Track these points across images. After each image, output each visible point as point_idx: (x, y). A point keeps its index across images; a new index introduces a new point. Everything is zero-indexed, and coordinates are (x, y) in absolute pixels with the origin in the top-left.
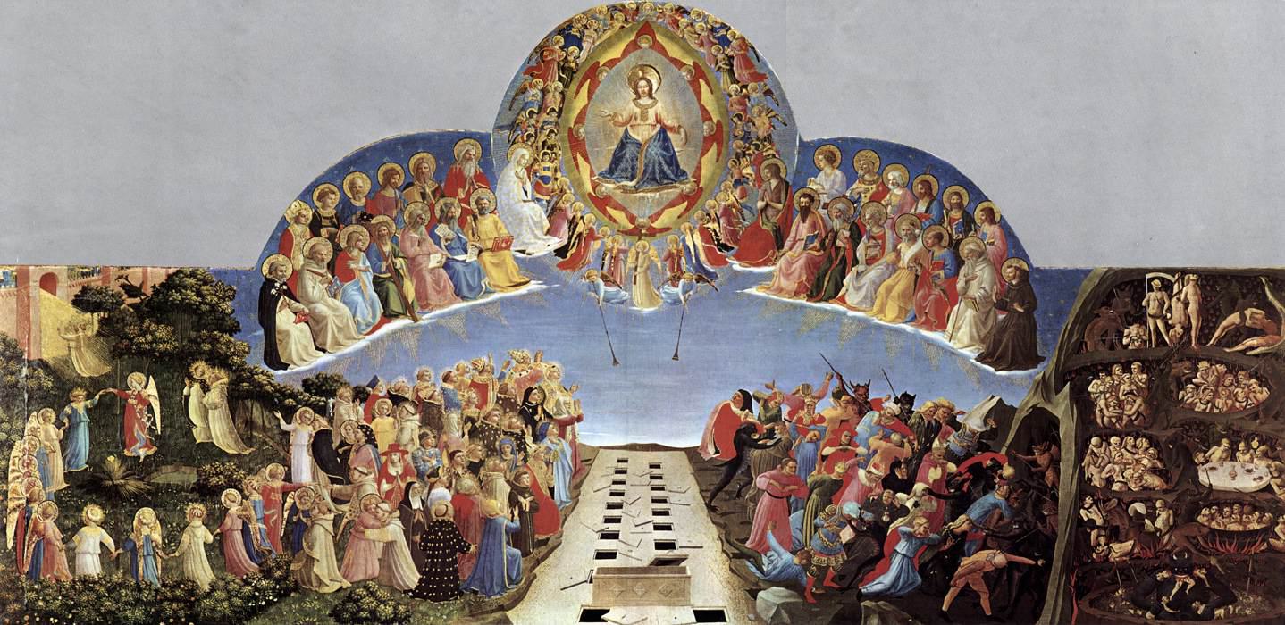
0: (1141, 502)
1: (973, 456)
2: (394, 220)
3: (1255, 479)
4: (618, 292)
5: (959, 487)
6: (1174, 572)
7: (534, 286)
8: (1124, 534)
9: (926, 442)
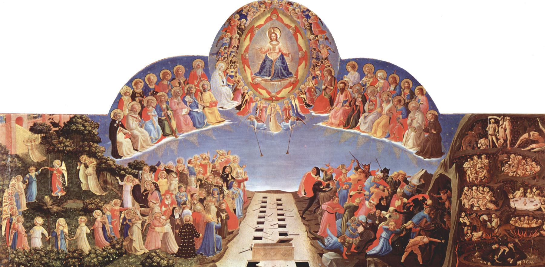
0: (486, 215)
1: (414, 195)
2: (167, 94)
3: (534, 205)
4: (263, 125)
5: (408, 208)
6: (500, 245)
7: (227, 122)
8: (478, 229)
9: (394, 190)
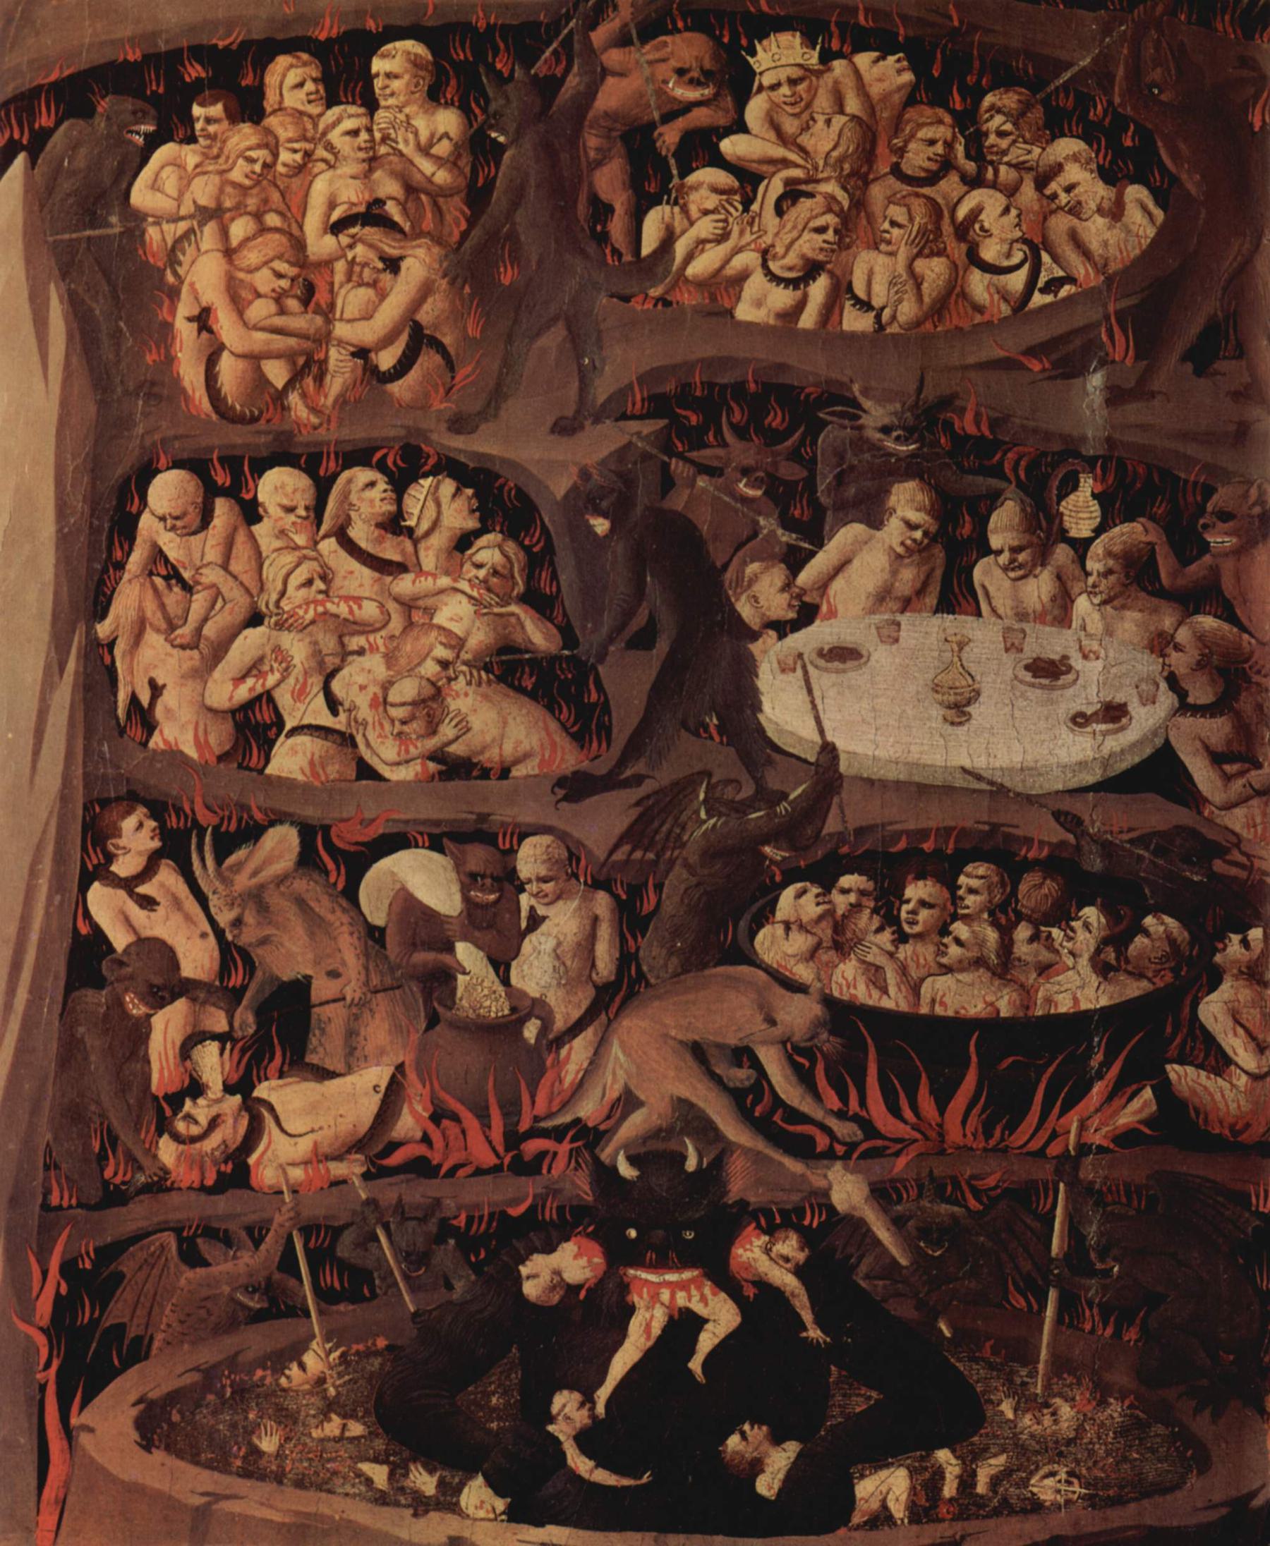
0: (436, 845)
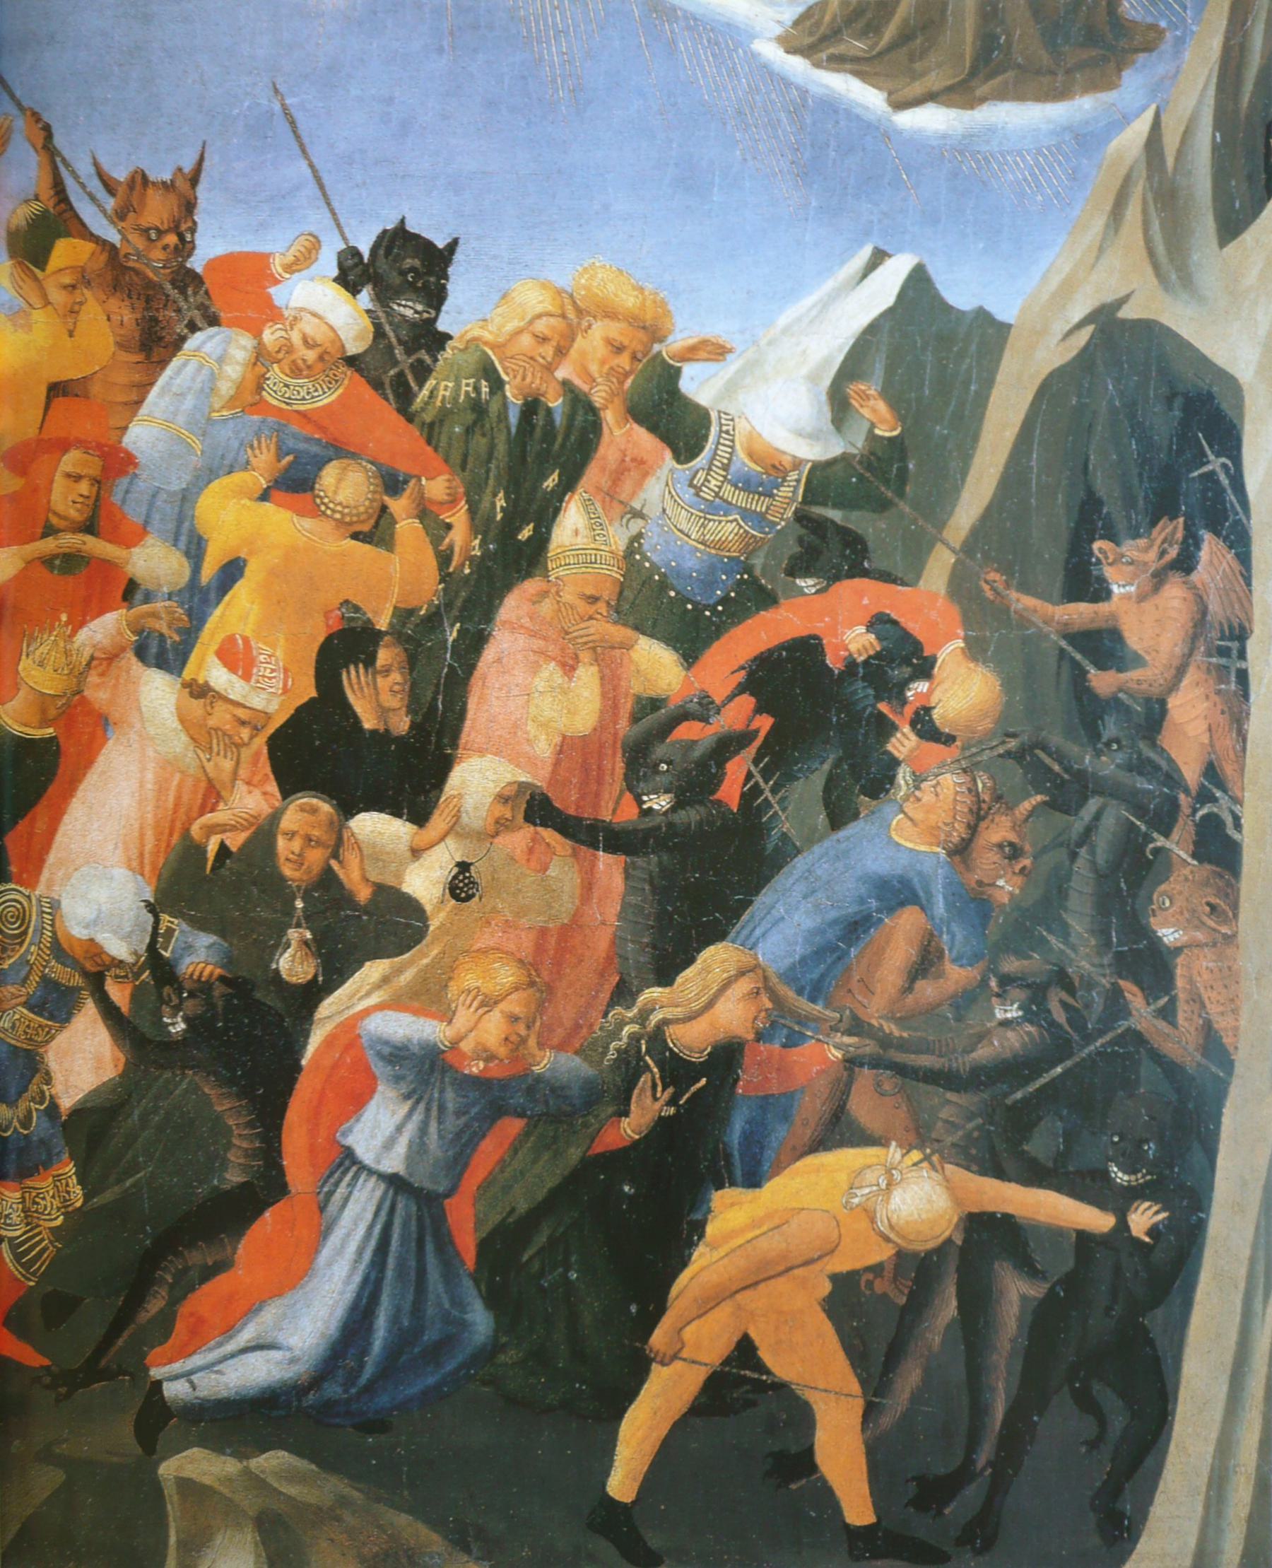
1: (767, 599)
9: (513, 519)
